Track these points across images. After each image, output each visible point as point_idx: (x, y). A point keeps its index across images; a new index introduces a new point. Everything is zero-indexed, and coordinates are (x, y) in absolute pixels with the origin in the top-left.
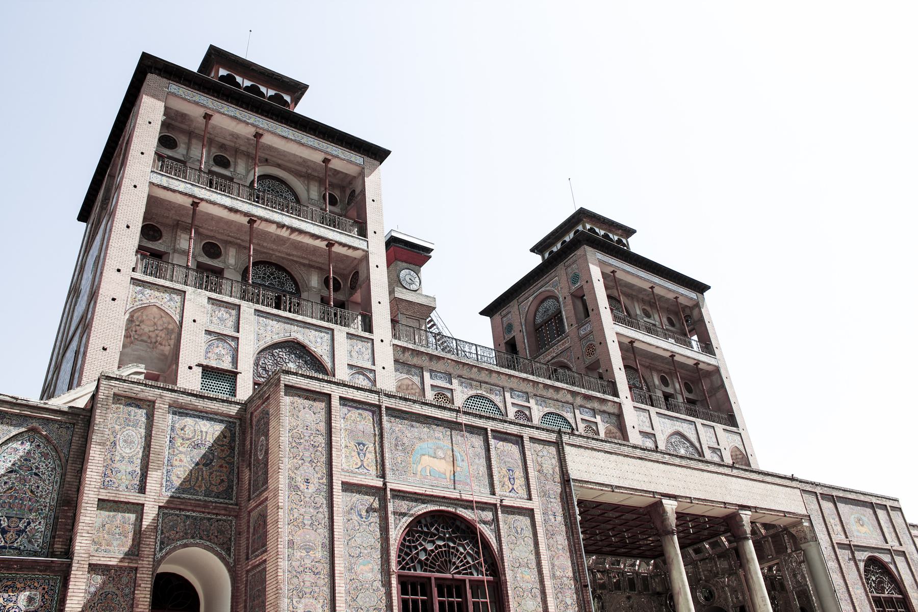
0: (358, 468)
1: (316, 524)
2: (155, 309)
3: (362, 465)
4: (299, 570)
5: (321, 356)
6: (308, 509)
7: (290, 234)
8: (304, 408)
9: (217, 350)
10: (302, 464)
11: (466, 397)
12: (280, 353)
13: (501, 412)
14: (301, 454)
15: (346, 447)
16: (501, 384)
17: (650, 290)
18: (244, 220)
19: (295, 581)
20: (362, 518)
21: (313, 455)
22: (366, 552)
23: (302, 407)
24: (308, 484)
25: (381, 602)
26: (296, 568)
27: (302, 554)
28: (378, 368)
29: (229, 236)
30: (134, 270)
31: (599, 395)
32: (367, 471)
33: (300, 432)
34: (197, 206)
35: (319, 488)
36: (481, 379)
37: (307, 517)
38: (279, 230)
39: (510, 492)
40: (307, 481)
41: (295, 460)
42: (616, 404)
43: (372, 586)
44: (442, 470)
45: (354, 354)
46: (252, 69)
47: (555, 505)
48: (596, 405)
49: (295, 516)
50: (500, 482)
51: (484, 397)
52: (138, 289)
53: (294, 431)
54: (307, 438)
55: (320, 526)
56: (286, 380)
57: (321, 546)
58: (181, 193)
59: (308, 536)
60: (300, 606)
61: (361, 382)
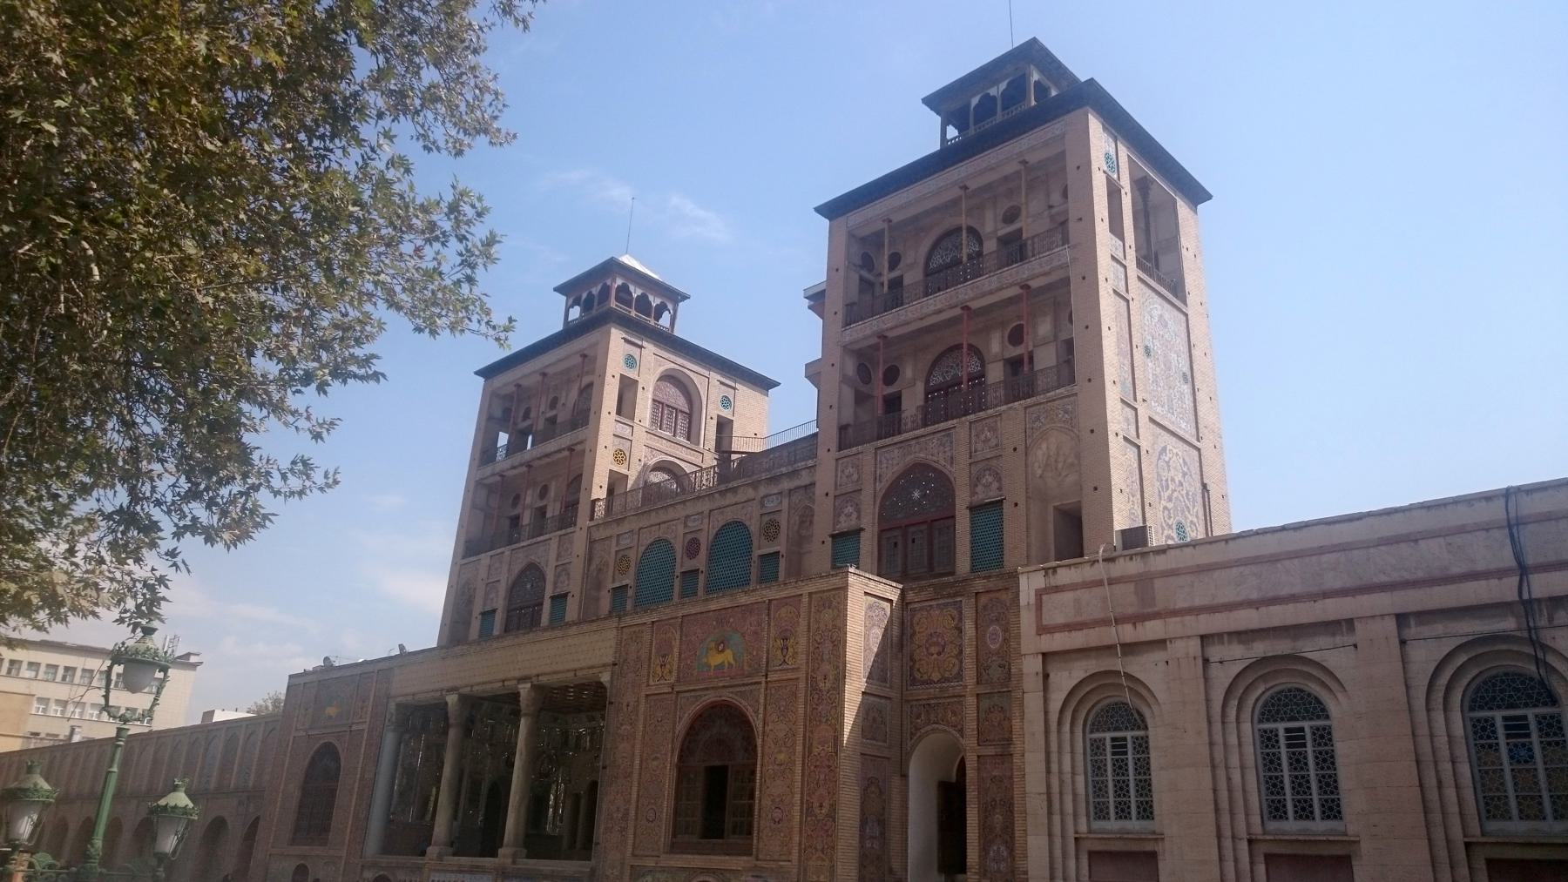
9: (491, 596)
16: (677, 516)
30: (464, 557)
36: (658, 521)
48: (786, 485)
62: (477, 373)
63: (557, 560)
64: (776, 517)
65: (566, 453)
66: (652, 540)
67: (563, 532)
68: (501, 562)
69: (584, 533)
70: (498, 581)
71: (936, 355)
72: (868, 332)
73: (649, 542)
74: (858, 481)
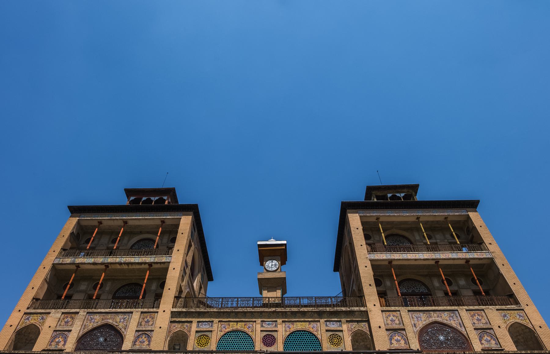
2: (33, 326)
5: (121, 329)
7: (128, 266)
9: (57, 340)
11: (222, 333)
12: (96, 333)
13: (251, 338)
16: (254, 320)
17: (417, 220)
18: (103, 267)
28: (157, 330)
29: (108, 276)
30: (28, 308)
31: (344, 309)
34: (80, 267)
38: (121, 266)
42: (363, 313)
45: (143, 323)
46: (146, 191)
51: (239, 331)
52: (26, 318)
58: (68, 264)
61: (143, 339)
62: (70, 207)
63: (137, 327)
64: (340, 334)
65: (147, 266)
66: (231, 329)
67: (146, 310)
68: (73, 318)
69: (168, 315)
70: (70, 331)
71: (401, 280)
72: (385, 258)
73: (228, 330)
74: (400, 324)
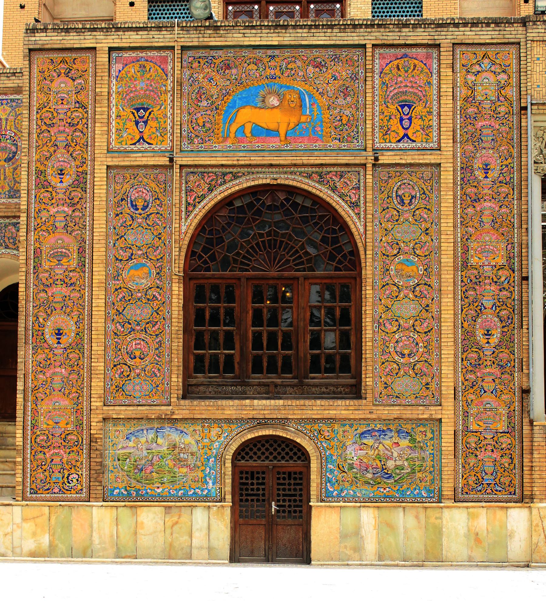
0: (135, 144)
1: (72, 225)
3: (142, 138)
4: (48, 283)
6: (61, 208)
8: (59, 76)
10: (55, 151)
14: (54, 139)
15: (118, 116)
19: (43, 295)
20: (137, 209)
21: (69, 138)
22: (140, 252)
23: (55, 74)
24: (62, 176)
25: (158, 314)
26: (44, 280)
27: (52, 264)
32: (147, 146)
33: (52, 110)
35: (78, 178)
37: (60, 217)
39: (399, 141)
40: (61, 173)
41: (45, 148)
43: (146, 295)
44: (273, 126)
47: (491, 152)
49: (44, 219)
50: (381, 127)
53: (45, 110)
54: (62, 116)
55: (77, 227)
56: (30, 42)
57: (77, 251)
59: (60, 242)
60: (49, 323)
